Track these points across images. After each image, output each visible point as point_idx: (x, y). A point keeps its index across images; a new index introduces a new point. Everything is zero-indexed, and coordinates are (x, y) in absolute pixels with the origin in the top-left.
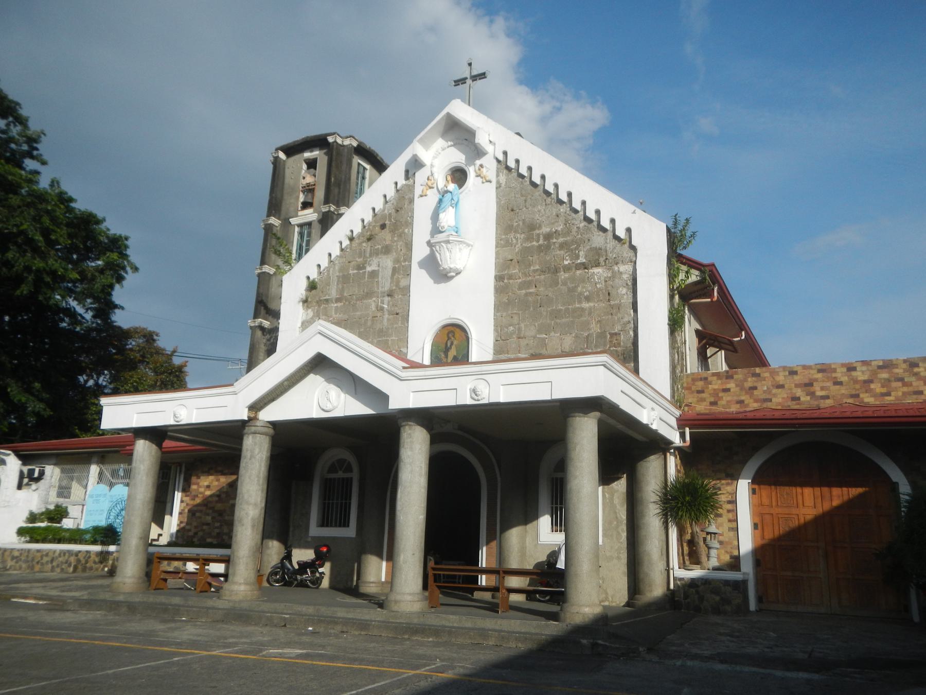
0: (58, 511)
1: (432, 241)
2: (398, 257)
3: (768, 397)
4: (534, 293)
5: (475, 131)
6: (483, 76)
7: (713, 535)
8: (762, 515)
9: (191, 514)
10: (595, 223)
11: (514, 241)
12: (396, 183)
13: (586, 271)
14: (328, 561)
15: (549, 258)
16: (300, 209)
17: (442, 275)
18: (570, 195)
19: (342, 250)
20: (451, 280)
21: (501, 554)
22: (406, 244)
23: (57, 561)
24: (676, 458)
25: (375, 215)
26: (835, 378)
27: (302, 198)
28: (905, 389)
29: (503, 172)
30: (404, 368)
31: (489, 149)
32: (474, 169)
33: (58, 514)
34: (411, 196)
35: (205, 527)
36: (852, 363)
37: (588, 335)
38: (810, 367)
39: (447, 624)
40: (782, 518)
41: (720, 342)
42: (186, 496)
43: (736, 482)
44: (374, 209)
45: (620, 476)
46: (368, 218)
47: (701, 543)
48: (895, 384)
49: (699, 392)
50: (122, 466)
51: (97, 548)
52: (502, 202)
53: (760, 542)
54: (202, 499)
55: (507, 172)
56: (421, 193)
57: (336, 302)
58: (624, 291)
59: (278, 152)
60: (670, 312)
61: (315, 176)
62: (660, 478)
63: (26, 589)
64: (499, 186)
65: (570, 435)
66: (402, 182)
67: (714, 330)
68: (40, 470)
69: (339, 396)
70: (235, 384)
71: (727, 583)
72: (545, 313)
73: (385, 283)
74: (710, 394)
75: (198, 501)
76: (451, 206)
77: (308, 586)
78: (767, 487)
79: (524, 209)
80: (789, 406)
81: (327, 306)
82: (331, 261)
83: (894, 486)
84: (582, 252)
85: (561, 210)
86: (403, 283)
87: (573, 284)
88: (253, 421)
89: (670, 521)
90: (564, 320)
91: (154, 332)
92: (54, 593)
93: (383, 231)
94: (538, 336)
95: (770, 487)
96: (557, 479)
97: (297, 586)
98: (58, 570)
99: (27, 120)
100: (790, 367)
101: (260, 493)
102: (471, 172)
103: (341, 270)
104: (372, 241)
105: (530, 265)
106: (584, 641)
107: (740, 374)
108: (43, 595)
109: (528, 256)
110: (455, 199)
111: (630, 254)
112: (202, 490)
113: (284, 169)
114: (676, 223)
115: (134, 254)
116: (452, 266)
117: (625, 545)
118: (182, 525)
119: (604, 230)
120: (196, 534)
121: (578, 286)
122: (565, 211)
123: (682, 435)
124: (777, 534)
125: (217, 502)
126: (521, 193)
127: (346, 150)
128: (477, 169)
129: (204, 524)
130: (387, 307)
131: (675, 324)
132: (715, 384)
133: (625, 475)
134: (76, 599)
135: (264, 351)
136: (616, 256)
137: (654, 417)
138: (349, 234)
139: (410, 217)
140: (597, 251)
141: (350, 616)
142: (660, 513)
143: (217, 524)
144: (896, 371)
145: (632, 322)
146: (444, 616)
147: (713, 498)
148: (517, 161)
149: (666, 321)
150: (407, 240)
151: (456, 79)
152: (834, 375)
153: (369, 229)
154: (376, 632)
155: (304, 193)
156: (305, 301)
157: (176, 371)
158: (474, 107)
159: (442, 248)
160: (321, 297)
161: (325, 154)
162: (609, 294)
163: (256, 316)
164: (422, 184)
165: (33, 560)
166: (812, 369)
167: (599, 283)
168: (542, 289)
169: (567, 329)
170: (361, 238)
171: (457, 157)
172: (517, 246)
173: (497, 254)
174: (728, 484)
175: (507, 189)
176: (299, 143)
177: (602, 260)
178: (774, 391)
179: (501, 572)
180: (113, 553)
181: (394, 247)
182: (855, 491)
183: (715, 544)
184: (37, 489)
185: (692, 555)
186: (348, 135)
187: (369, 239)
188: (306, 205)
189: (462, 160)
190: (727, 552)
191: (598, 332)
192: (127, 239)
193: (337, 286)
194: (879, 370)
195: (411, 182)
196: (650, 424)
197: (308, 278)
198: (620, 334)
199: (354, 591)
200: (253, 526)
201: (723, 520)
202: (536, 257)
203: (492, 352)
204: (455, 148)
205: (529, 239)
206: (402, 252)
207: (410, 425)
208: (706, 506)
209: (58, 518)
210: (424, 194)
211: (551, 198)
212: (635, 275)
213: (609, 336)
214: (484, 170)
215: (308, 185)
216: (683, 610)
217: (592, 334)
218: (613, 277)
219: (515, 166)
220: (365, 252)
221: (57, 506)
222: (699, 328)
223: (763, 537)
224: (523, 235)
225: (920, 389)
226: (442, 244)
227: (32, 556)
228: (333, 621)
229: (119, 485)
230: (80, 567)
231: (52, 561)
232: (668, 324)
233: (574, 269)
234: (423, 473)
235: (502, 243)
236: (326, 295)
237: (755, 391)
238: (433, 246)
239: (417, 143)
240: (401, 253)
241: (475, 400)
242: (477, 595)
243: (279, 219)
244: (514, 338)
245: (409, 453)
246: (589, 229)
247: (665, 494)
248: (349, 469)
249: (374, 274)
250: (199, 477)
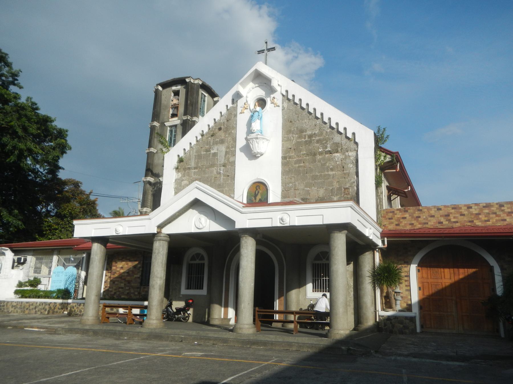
0: (36, 281)
1: (248, 138)
2: (228, 146)
3: (426, 222)
4: (303, 166)
5: (271, 79)
6: (273, 49)
7: (398, 293)
8: (423, 283)
9: (112, 283)
10: (336, 130)
11: (292, 138)
12: (227, 106)
13: (331, 155)
14: (191, 307)
15: (311, 147)
16: (170, 117)
17: (252, 155)
18: (322, 114)
19: (197, 141)
20: (256, 159)
21: (287, 304)
22: (233, 139)
23: (38, 308)
24: (379, 253)
25: (215, 122)
26: (461, 212)
27: (171, 112)
28: (497, 218)
29: (286, 102)
30: (243, 207)
31: (278, 88)
32: (270, 99)
33: (35, 282)
34: (236, 113)
35: (120, 290)
36: (470, 205)
37: (332, 189)
38: (448, 207)
39: (269, 340)
40: (433, 284)
41: (398, 192)
42: (108, 273)
43: (409, 266)
44: (215, 120)
45: (350, 263)
46: (212, 124)
47: (393, 298)
48: (491, 216)
49: (390, 219)
50: (71, 256)
51: (60, 301)
52: (285, 117)
53: (422, 297)
54: (118, 274)
55: (288, 101)
56: (241, 111)
57: (194, 169)
58: (351, 166)
59: (158, 86)
60: (376, 177)
61: (179, 100)
62: (371, 264)
63: (27, 323)
64: (283, 109)
65: (332, 242)
66: (230, 105)
67: (394, 186)
68: (24, 258)
69: (206, 221)
70: (150, 214)
71: (406, 318)
72: (309, 177)
73: (221, 159)
74: (396, 220)
75: (116, 275)
76: (258, 119)
77: (181, 321)
78: (425, 268)
79: (297, 121)
80: (437, 226)
81: (189, 171)
82: (191, 147)
83: (491, 269)
84: (329, 145)
85: (317, 122)
86: (231, 160)
87: (324, 161)
88: (160, 234)
89: (377, 286)
90: (319, 181)
91: (80, 182)
92: (46, 325)
93: (220, 131)
94: (305, 189)
95: (427, 269)
96: (316, 264)
97: (175, 321)
98: (39, 313)
99: (11, 64)
100: (437, 206)
101: (163, 272)
102: (268, 101)
103: (196, 152)
104: (214, 136)
105: (301, 152)
106: (343, 348)
107: (411, 209)
108: (42, 326)
109: (299, 147)
110: (260, 115)
111: (354, 146)
112: (118, 269)
113: (161, 95)
114: (379, 131)
115: (70, 140)
116: (259, 151)
117: (352, 299)
118: (107, 288)
119: (340, 133)
120: (115, 293)
121: (327, 163)
122: (319, 123)
123: (383, 242)
124: (431, 293)
125: (127, 276)
126: (296, 113)
127: (196, 86)
128: (271, 99)
129: (120, 288)
130: (222, 172)
131: (378, 184)
132: (398, 215)
133: (352, 262)
134: (63, 328)
135: (151, 195)
136: (347, 147)
137: (371, 233)
138: (201, 132)
139: (235, 124)
140: (337, 145)
141: (216, 336)
142: (371, 282)
143: (127, 288)
144: (492, 209)
145: (356, 182)
146: (267, 335)
147: (399, 274)
148: (294, 96)
149: (374, 182)
150: (233, 136)
151: (258, 50)
152: (460, 211)
153: (212, 130)
154: (232, 344)
155: (172, 109)
156: (177, 168)
157: (92, 203)
158: (268, 66)
159: (253, 141)
160: (186, 166)
161: (184, 88)
162: (343, 167)
163: (146, 175)
164: (242, 107)
166: (449, 207)
167: (338, 161)
168: (307, 164)
169: (321, 185)
170: (208, 135)
171: (260, 93)
172: (294, 141)
173: (283, 145)
174: (405, 267)
175: (288, 110)
176: (170, 81)
177: (339, 149)
178: (429, 219)
179: (294, 313)
180: (70, 303)
181: (226, 140)
182: (471, 271)
183: (399, 298)
184: (23, 269)
185: (388, 303)
186: (197, 78)
187: (212, 136)
188: (174, 115)
189: (263, 94)
190: (405, 302)
191: (338, 187)
192: (67, 131)
193: (195, 161)
194: (484, 208)
195: (236, 105)
196: (369, 236)
197: (179, 156)
198: (349, 188)
199: (208, 323)
200: (160, 289)
201: (403, 285)
202: (304, 147)
203: (280, 197)
204: (259, 88)
205: (300, 137)
206: (231, 143)
207: (246, 237)
208: (395, 278)
209: (35, 284)
210: (242, 112)
211: (312, 116)
212: (357, 158)
213: (343, 189)
214: (275, 100)
215: (175, 104)
216: (383, 332)
217: (334, 188)
218: (346, 158)
219: (292, 99)
220: (210, 142)
221: (35, 278)
222: (388, 185)
223: (423, 294)
224: (297, 135)
225: (505, 218)
226: (253, 139)
227: (24, 305)
228: (209, 339)
229: (71, 267)
230: (51, 311)
231: (35, 308)
232: (375, 184)
233: (324, 154)
234: (253, 262)
235: (285, 139)
236: (189, 165)
237: (419, 218)
238: (249, 140)
239: (239, 85)
240: (230, 143)
241: (282, 224)
242: (274, 325)
243: (159, 123)
244: (292, 190)
245: (246, 251)
246: (333, 133)
247: (374, 272)
248: (202, 258)
249: (215, 154)
250: (116, 263)
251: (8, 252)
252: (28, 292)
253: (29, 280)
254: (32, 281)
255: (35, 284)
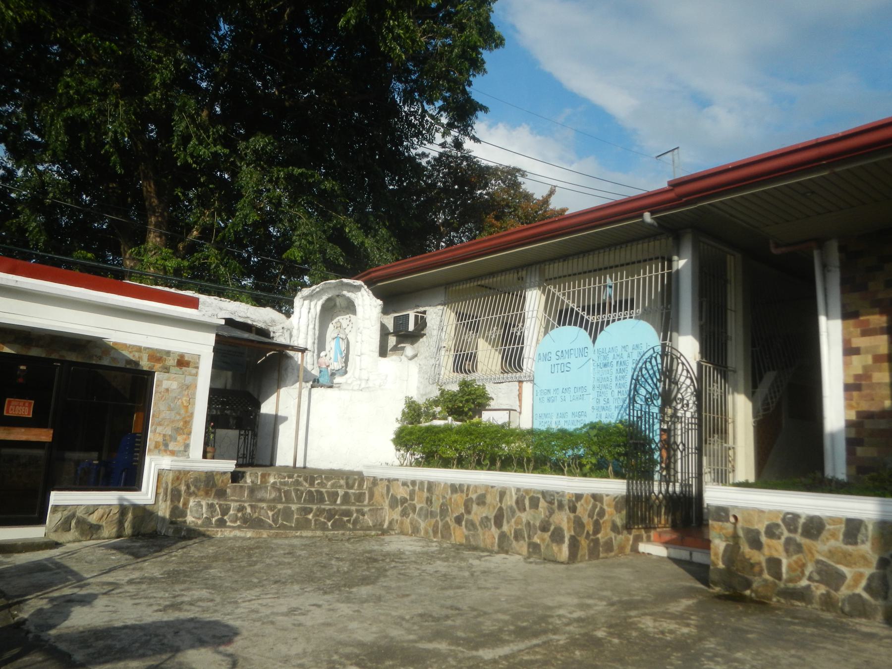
42: (866, 333)
68: (416, 317)
165: (444, 511)
184: (416, 356)
209: (470, 410)
230: (584, 543)
231: (499, 520)
251: (362, 296)
252: (455, 437)
253: (443, 393)
254: (454, 395)
255: (470, 410)
